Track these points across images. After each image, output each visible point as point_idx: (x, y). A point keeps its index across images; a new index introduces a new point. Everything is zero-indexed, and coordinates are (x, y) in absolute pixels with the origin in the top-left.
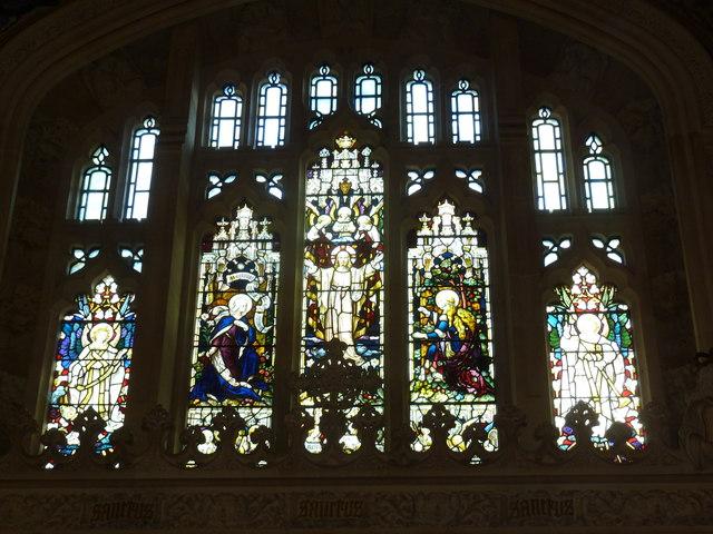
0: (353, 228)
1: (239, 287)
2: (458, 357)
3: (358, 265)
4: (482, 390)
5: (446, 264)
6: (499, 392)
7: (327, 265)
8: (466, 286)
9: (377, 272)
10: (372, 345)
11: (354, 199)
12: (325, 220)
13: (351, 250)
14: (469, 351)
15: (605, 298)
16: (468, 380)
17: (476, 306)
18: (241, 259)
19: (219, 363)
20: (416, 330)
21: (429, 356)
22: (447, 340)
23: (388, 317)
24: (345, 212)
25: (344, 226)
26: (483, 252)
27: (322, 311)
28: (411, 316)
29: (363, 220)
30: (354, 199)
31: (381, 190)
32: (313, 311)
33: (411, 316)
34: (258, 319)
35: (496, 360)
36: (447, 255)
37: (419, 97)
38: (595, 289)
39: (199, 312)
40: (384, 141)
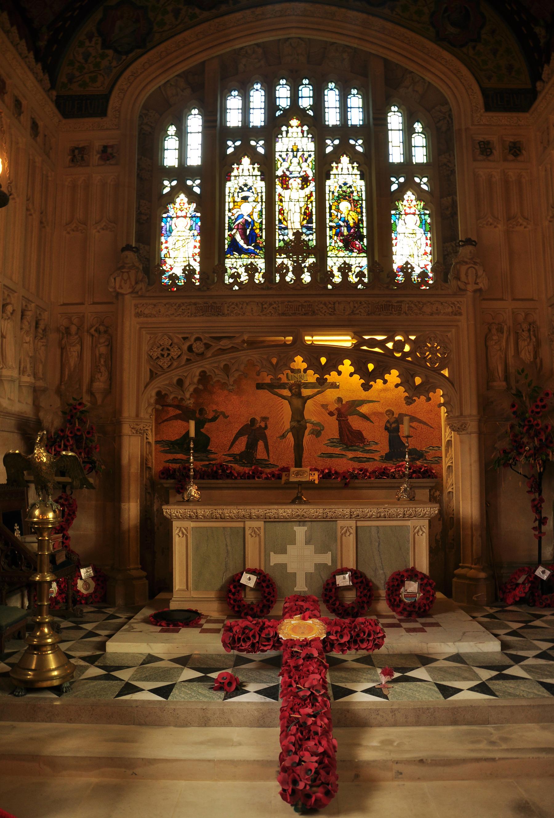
0: (299, 169)
1: (245, 199)
2: (350, 235)
3: (302, 188)
4: (360, 251)
5: (344, 189)
6: (369, 252)
7: (287, 188)
8: (354, 200)
9: (312, 192)
10: (310, 229)
11: (299, 154)
12: (286, 165)
13: (299, 181)
14: (355, 232)
15: (419, 207)
16: (354, 246)
17: (359, 210)
18: (246, 185)
19: (238, 237)
20: (331, 221)
21: (337, 234)
22: (345, 226)
24: (295, 161)
25: (294, 168)
26: (362, 183)
27: (286, 212)
28: (328, 215)
29: (304, 165)
30: (299, 154)
31: (313, 149)
32: (281, 212)
33: (328, 215)
34: (255, 217)
35: (368, 237)
36: (345, 184)
37: (332, 97)
38: (414, 203)
39: (227, 212)
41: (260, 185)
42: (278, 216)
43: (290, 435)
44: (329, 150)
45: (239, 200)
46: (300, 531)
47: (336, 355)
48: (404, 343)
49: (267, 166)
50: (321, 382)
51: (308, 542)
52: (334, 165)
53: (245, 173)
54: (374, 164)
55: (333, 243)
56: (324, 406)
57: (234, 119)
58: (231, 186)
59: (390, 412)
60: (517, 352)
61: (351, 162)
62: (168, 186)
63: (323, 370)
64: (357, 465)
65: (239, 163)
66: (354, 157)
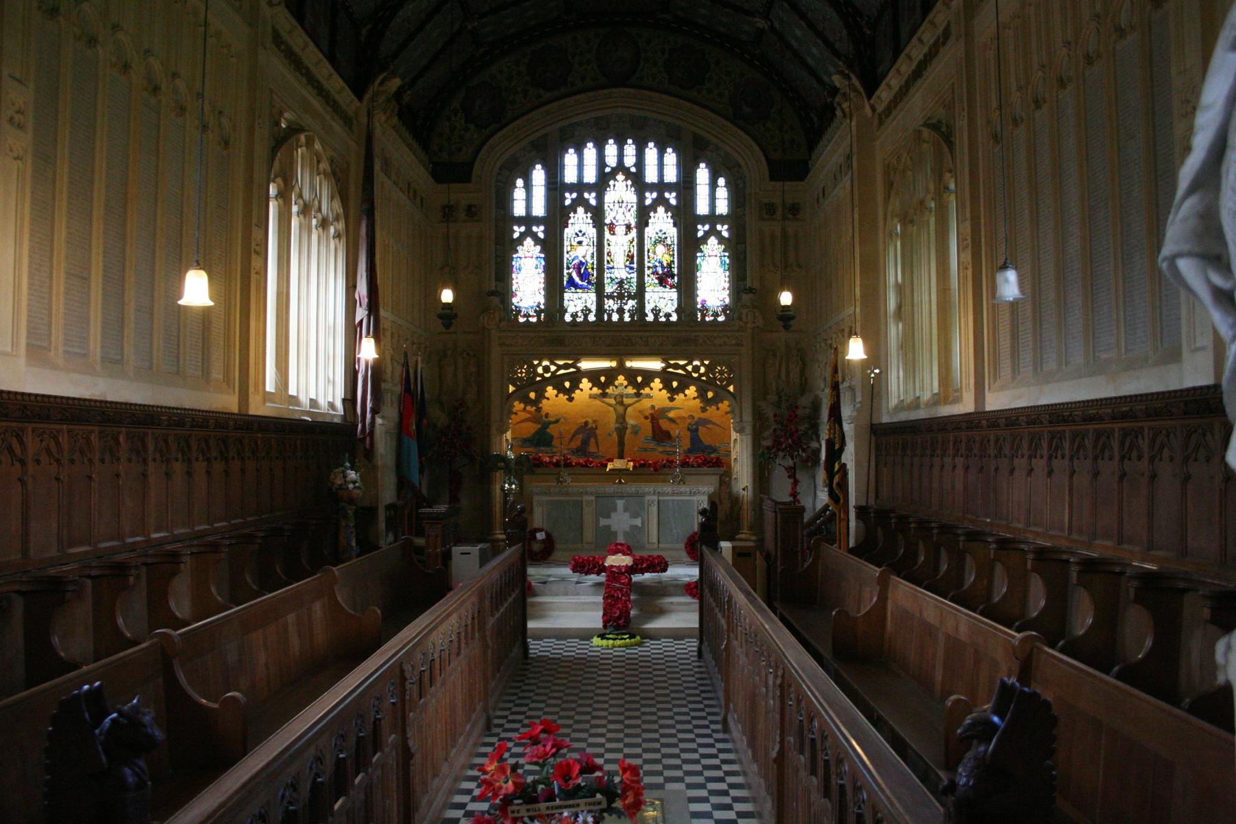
1: (580, 243)
4: (672, 287)
6: (678, 287)
10: (632, 268)
13: (624, 228)
16: (667, 282)
19: (574, 275)
23: (638, 259)
24: (621, 211)
25: (620, 217)
26: (675, 230)
29: (628, 214)
34: (588, 258)
37: (651, 153)
40: (637, 179)
41: (592, 232)
42: (606, 258)
43: (615, 435)
44: (648, 202)
45: (575, 243)
46: (620, 503)
47: (649, 376)
48: (698, 367)
49: (598, 215)
50: (638, 395)
51: (626, 510)
52: (652, 214)
53: (580, 221)
54: (685, 216)
55: (650, 280)
57: (570, 176)
58: (569, 232)
59: (692, 417)
61: (666, 212)
62: (518, 230)
63: (639, 387)
64: (665, 457)
65: (575, 212)
66: (668, 207)
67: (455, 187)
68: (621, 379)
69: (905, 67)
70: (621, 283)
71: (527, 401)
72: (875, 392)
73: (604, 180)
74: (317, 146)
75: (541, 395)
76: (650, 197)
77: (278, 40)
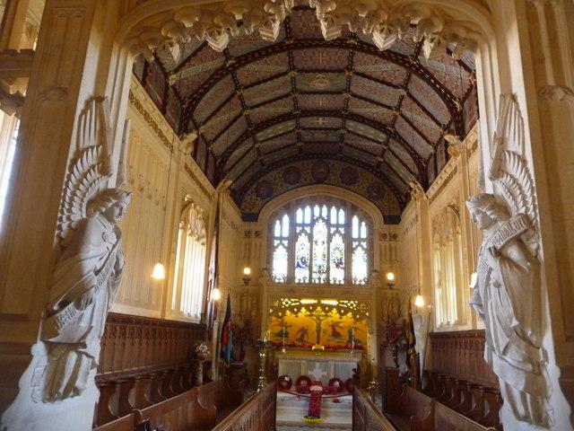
6: (344, 269)
23: (327, 256)
40: (328, 222)
41: (308, 244)
46: (318, 365)
47: (331, 307)
48: (353, 304)
49: (310, 237)
53: (303, 239)
54: (348, 239)
55: (332, 265)
56: (328, 323)
57: (299, 220)
60: (392, 307)
66: (341, 234)
67: (252, 223)
68: (319, 308)
69: (439, 181)
70: (320, 267)
71: (278, 317)
72: (431, 316)
73: (313, 222)
74: (198, 208)
75: (284, 314)
76: (333, 230)
77: (186, 167)
